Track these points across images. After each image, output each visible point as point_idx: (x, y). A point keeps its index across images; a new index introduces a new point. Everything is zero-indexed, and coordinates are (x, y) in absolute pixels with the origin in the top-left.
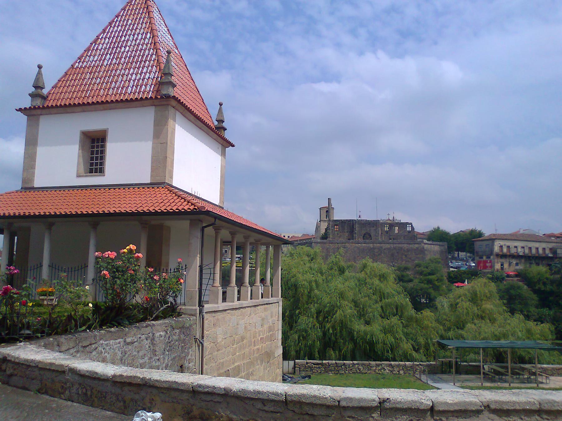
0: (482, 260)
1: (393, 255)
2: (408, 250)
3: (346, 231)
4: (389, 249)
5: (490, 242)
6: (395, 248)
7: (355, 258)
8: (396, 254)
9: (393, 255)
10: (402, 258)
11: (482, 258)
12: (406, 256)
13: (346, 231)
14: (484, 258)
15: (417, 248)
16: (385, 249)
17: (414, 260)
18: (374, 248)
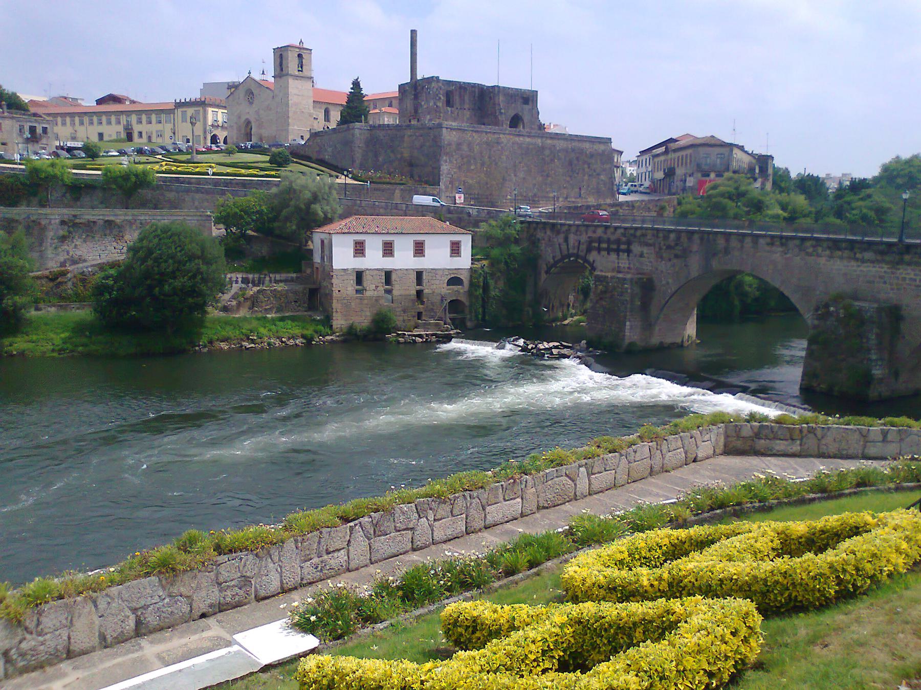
0: (707, 179)
1: (570, 163)
2: (592, 156)
3: (466, 106)
4: (566, 151)
5: (728, 149)
6: (573, 150)
7: (515, 166)
8: (575, 162)
9: (570, 163)
10: (584, 170)
11: (708, 176)
12: (589, 164)
13: (466, 106)
14: (712, 175)
15: (604, 152)
16: (559, 151)
17: (598, 175)
18: (543, 148)
